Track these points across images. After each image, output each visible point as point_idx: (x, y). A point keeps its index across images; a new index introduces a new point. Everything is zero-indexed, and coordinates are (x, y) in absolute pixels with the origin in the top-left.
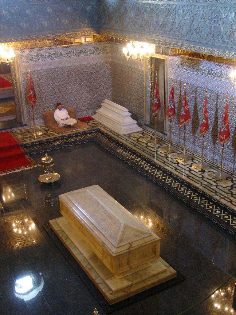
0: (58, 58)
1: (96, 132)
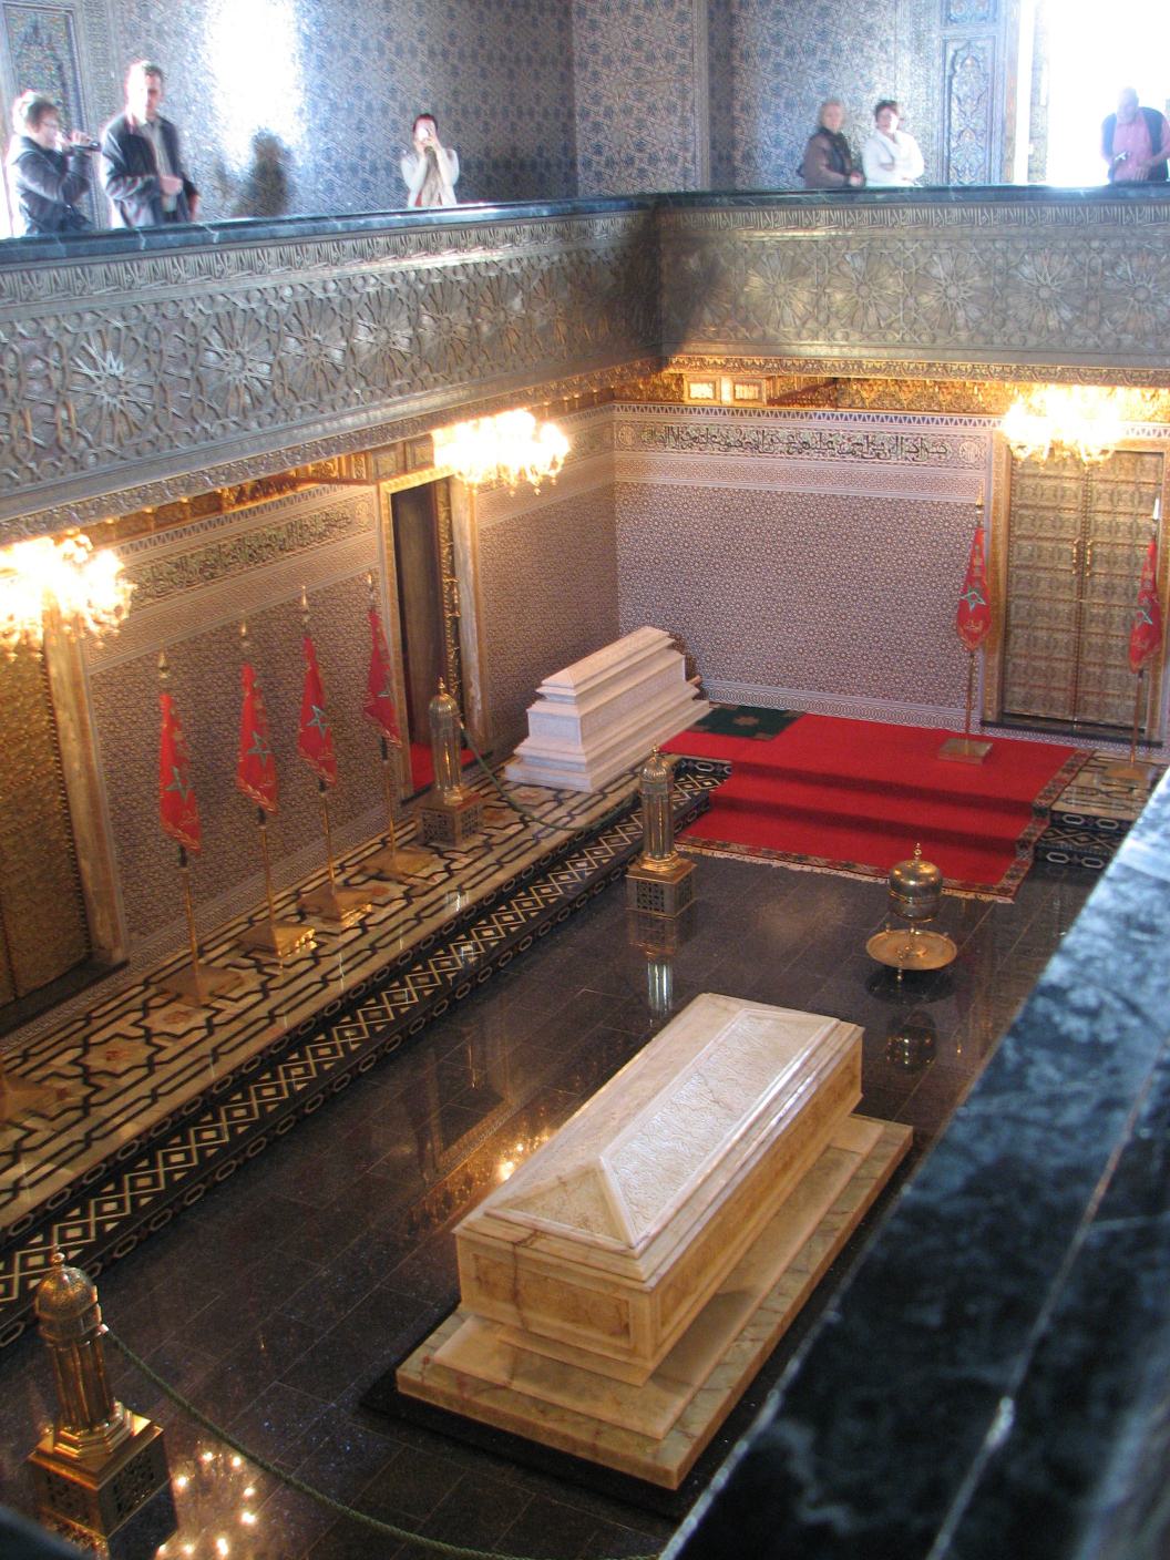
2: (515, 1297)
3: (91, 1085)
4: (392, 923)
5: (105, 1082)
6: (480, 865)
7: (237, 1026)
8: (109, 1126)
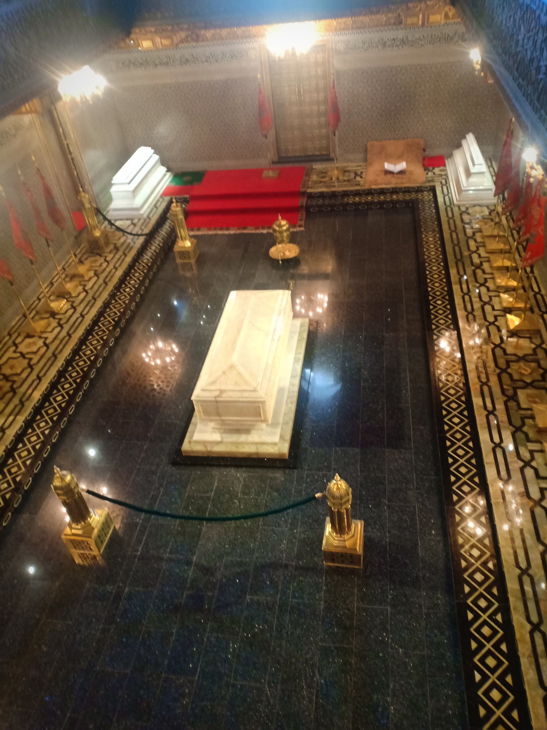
0: (400, 47)
1: (428, 191)
2: (218, 414)
3: (10, 381)
4: (96, 287)
5: (15, 378)
6: (117, 256)
7: (57, 342)
8: (28, 394)
